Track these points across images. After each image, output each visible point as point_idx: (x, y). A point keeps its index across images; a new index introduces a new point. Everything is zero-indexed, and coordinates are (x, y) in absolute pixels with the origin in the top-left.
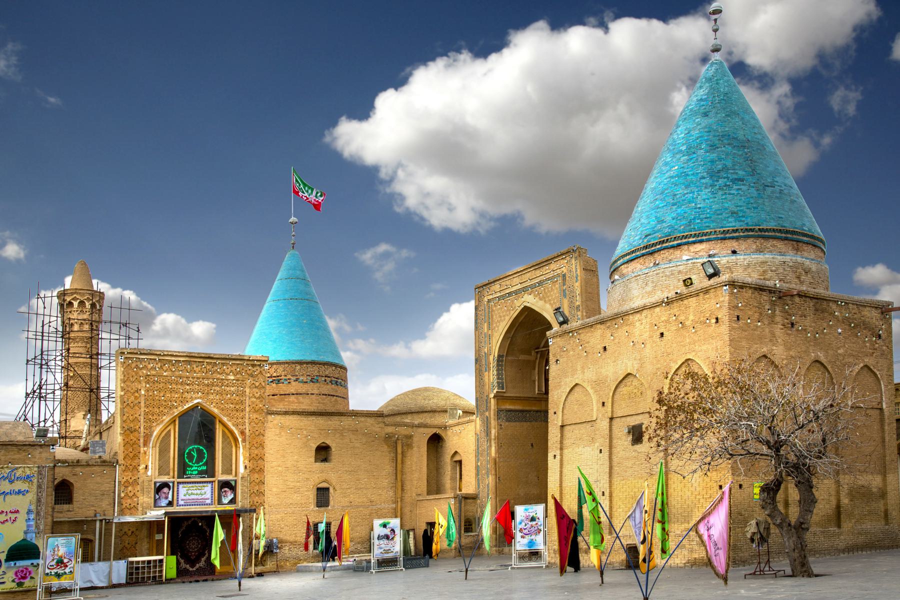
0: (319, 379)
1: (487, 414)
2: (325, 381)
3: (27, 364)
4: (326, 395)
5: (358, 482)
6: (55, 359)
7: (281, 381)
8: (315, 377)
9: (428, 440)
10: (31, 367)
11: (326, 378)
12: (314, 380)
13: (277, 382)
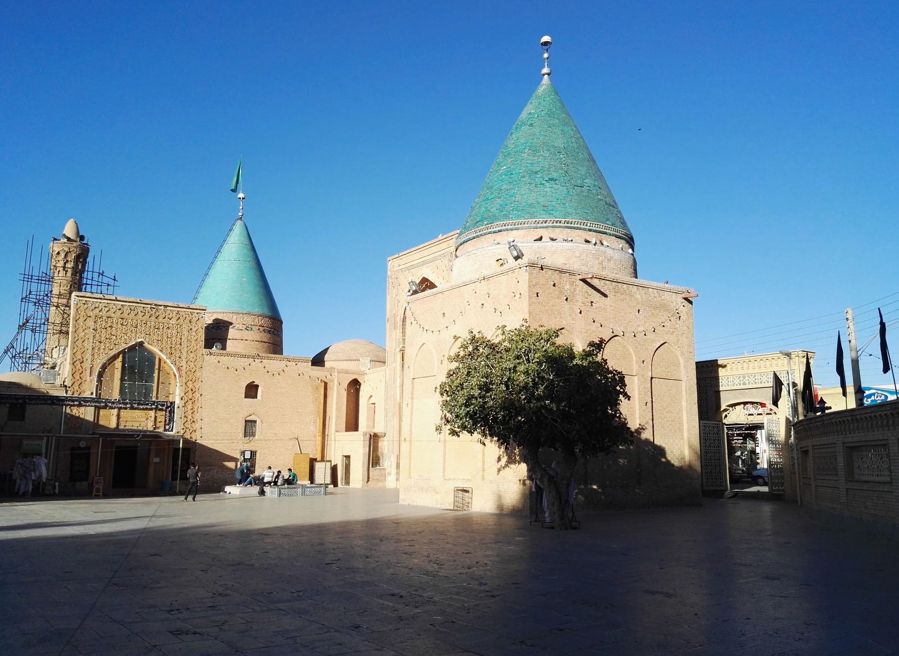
0: (254, 328)
1: (394, 365)
2: (259, 329)
3: (21, 301)
4: (259, 341)
5: (283, 417)
6: (43, 298)
7: (220, 327)
8: (250, 326)
9: (348, 384)
10: (23, 303)
11: (260, 327)
12: (248, 329)
13: (216, 328)
